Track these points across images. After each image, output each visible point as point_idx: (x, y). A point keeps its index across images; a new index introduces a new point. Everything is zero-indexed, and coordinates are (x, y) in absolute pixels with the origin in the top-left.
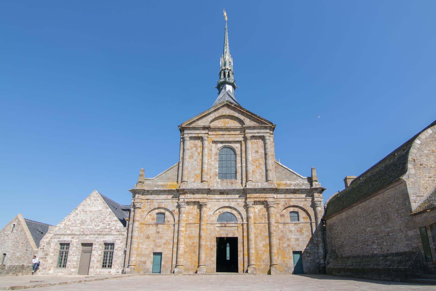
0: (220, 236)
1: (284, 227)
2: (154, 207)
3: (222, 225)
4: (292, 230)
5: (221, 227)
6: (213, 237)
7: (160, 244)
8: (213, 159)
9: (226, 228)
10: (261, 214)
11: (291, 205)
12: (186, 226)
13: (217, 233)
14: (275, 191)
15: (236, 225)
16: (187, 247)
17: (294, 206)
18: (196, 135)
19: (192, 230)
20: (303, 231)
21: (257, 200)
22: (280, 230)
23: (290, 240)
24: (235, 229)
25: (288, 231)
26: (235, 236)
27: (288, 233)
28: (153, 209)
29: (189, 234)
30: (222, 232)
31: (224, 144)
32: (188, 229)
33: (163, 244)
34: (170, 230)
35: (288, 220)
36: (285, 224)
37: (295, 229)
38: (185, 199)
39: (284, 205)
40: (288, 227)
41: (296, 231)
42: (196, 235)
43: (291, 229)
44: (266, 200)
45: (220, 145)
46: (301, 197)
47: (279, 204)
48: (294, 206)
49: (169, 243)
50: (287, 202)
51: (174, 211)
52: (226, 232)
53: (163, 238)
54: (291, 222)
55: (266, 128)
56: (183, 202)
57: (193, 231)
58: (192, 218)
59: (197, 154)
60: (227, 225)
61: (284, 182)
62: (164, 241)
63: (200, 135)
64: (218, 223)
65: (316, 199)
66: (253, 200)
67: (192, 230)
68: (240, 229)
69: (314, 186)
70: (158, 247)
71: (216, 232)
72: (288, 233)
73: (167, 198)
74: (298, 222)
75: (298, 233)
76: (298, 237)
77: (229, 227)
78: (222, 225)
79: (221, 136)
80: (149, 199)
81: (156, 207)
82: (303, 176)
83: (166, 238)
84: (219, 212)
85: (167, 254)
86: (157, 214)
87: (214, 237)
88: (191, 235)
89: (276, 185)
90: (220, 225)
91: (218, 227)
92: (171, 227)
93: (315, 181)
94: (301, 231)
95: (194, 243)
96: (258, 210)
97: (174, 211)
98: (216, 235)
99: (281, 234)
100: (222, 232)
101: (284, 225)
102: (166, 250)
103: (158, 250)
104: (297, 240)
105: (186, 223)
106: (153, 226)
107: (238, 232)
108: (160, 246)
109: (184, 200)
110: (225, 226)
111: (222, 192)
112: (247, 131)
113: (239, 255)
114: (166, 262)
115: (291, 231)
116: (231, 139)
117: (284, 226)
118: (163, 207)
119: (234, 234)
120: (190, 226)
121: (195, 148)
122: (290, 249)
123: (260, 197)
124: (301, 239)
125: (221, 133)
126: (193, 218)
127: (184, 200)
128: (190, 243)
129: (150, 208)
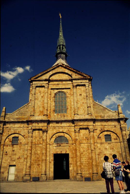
0: (56, 153)
2: (11, 133)
3: (58, 145)
8: (51, 100)
9: (61, 147)
11: (105, 130)
14: (94, 121)
15: (68, 145)
17: (107, 131)
18: (41, 85)
21: (82, 127)
22: (98, 148)
26: (67, 153)
28: (10, 134)
31: (59, 90)
35: (104, 140)
36: (101, 143)
38: (32, 127)
39: (100, 131)
44: (88, 127)
45: (56, 91)
46: (111, 125)
47: (97, 129)
48: (107, 131)
50: (102, 128)
51: (25, 135)
52: (61, 150)
54: (106, 142)
55: (86, 79)
56: (31, 129)
59: (41, 97)
60: (61, 145)
61: (100, 115)
63: (43, 85)
65: (122, 126)
66: (79, 127)
69: (120, 117)
70: (13, 161)
73: (20, 126)
74: (111, 142)
77: (63, 146)
78: (58, 145)
79: (57, 85)
80: (8, 128)
81: (12, 133)
82: (113, 110)
84: (56, 136)
86: (13, 137)
87: (52, 153)
89: (94, 116)
90: (56, 145)
91: (55, 146)
93: (120, 113)
96: (83, 134)
97: (25, 135)
99: (99, 151)
100: (58, 150)
101: (101, 144)
106: (10, 146)
108: (14, 161)
109: (32, 128)
111: (57, 122)
112: (74, 81)
113: (70, 167)
116: (63, 87)
117: (101, 145)
118: (17, 133)
119: (66, 152)
121: (39, 93)
123: (84, 125)
125: (57, 83)
127: (32, 128)
129: (8, 134)
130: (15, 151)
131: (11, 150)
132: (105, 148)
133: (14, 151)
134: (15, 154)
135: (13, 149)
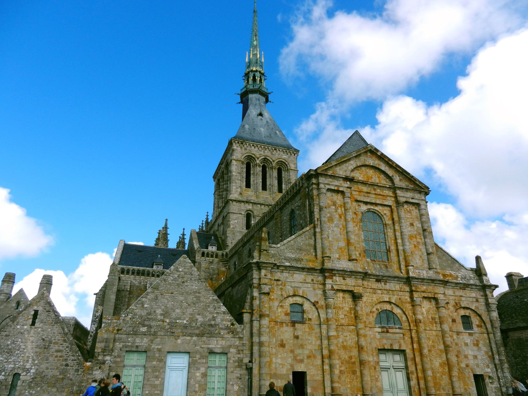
1: (458, 338)
4: (467, 343)
5: (382, 332)
6: (374, 348)
7: (302, 358)
9: (388, 335)
10: (430, 317)
12: (337, 328)
13: (378, 343)
15: (401, 331)
16: (342, 363)
19: (346, 336)
20: (480, 345)
23: (468, 358)
24: (400, 337)
25: (463, 344)
27: (464, 348)
29: (343, 342)
30: (385, 341)
32: (340, 333)
33: (306, 358)
34: (314, 334)
37: (470, 341)
40: (463, 338)
41: (472, 345)
42: (352, 344)
43: (466, 342)
49: (315, 357)
53: (305, 347)
57: (348, 338)
58: (343, 316)
60: (390, 331)
62: (307, 352)
64: (377, 326)
67: (346, 336)
68: (407, 338)
70: (299, 362)
71: (377, 341)
72: (464, 348)
75: (475, 348)
76: (476, 353)
83: (309, 347)
85: (314, 375)
87: (375, 348)
88: (345, 344)
92: (314, 329)
94: (477, 345)
95: (351, 358)
96: (426, 311)
98: (377, 345)
100: (385, 341)
102: (311, 367)
103: (299, 368)
104: (475, 357)
105: (337, 324)
107: (405, 342)
108: (302, 361)
110: (387, 332)
114: (314, 388)
115: (466, 344)
119: (400, 345)
120: (343, 329)
122: (470, 371)
124: (479, 357)
126: (345, 316)
128: (347, 357)
130: (300, 337)
131: (292, 335)
132: (464, 343)
133: (297, 337)
134: (302, 346)
135: (296, 334)
